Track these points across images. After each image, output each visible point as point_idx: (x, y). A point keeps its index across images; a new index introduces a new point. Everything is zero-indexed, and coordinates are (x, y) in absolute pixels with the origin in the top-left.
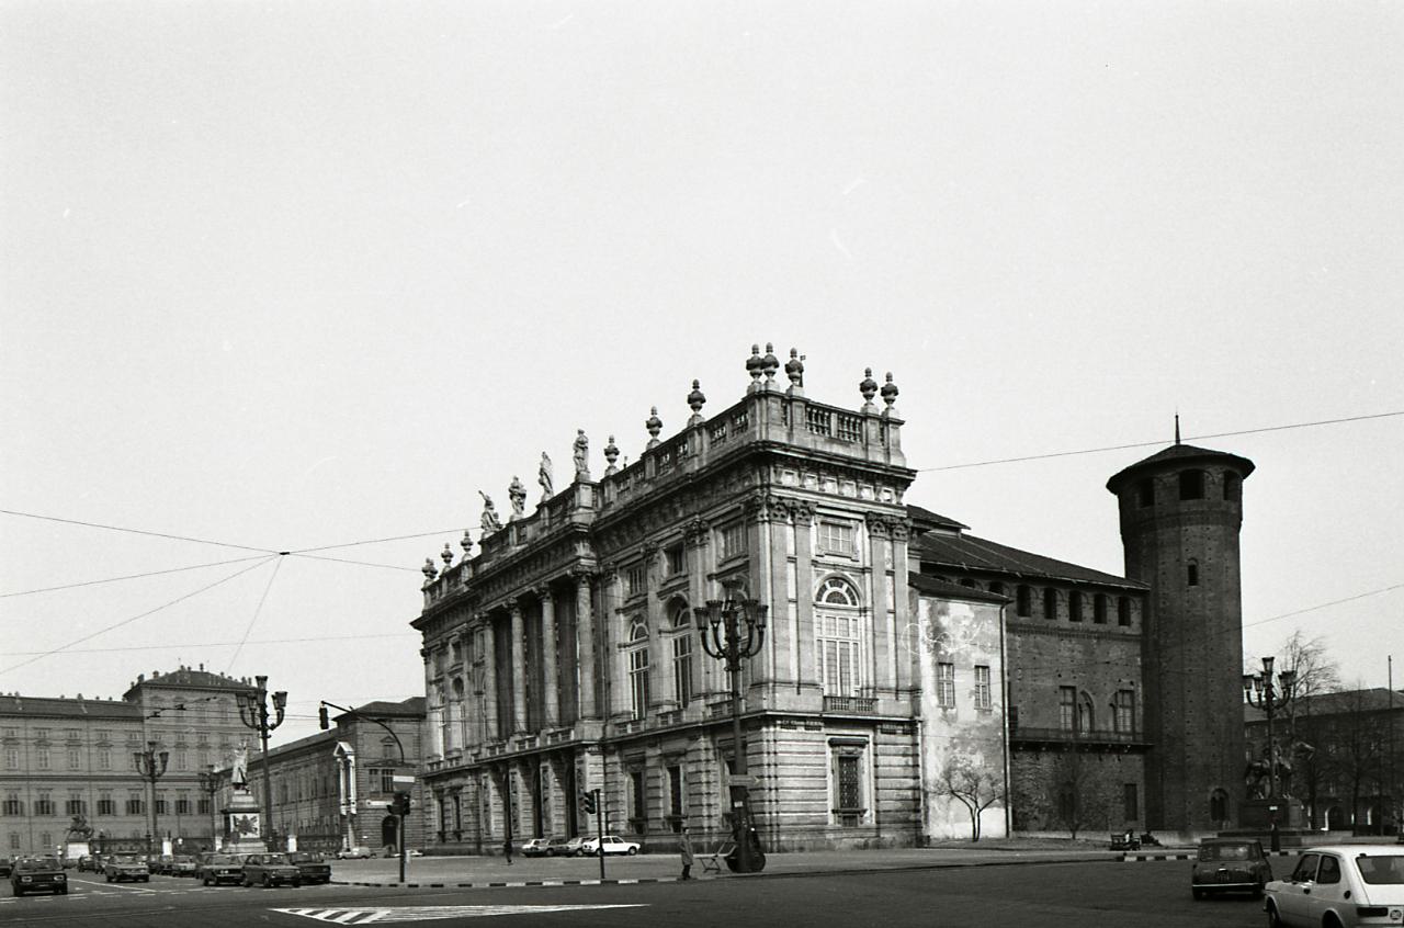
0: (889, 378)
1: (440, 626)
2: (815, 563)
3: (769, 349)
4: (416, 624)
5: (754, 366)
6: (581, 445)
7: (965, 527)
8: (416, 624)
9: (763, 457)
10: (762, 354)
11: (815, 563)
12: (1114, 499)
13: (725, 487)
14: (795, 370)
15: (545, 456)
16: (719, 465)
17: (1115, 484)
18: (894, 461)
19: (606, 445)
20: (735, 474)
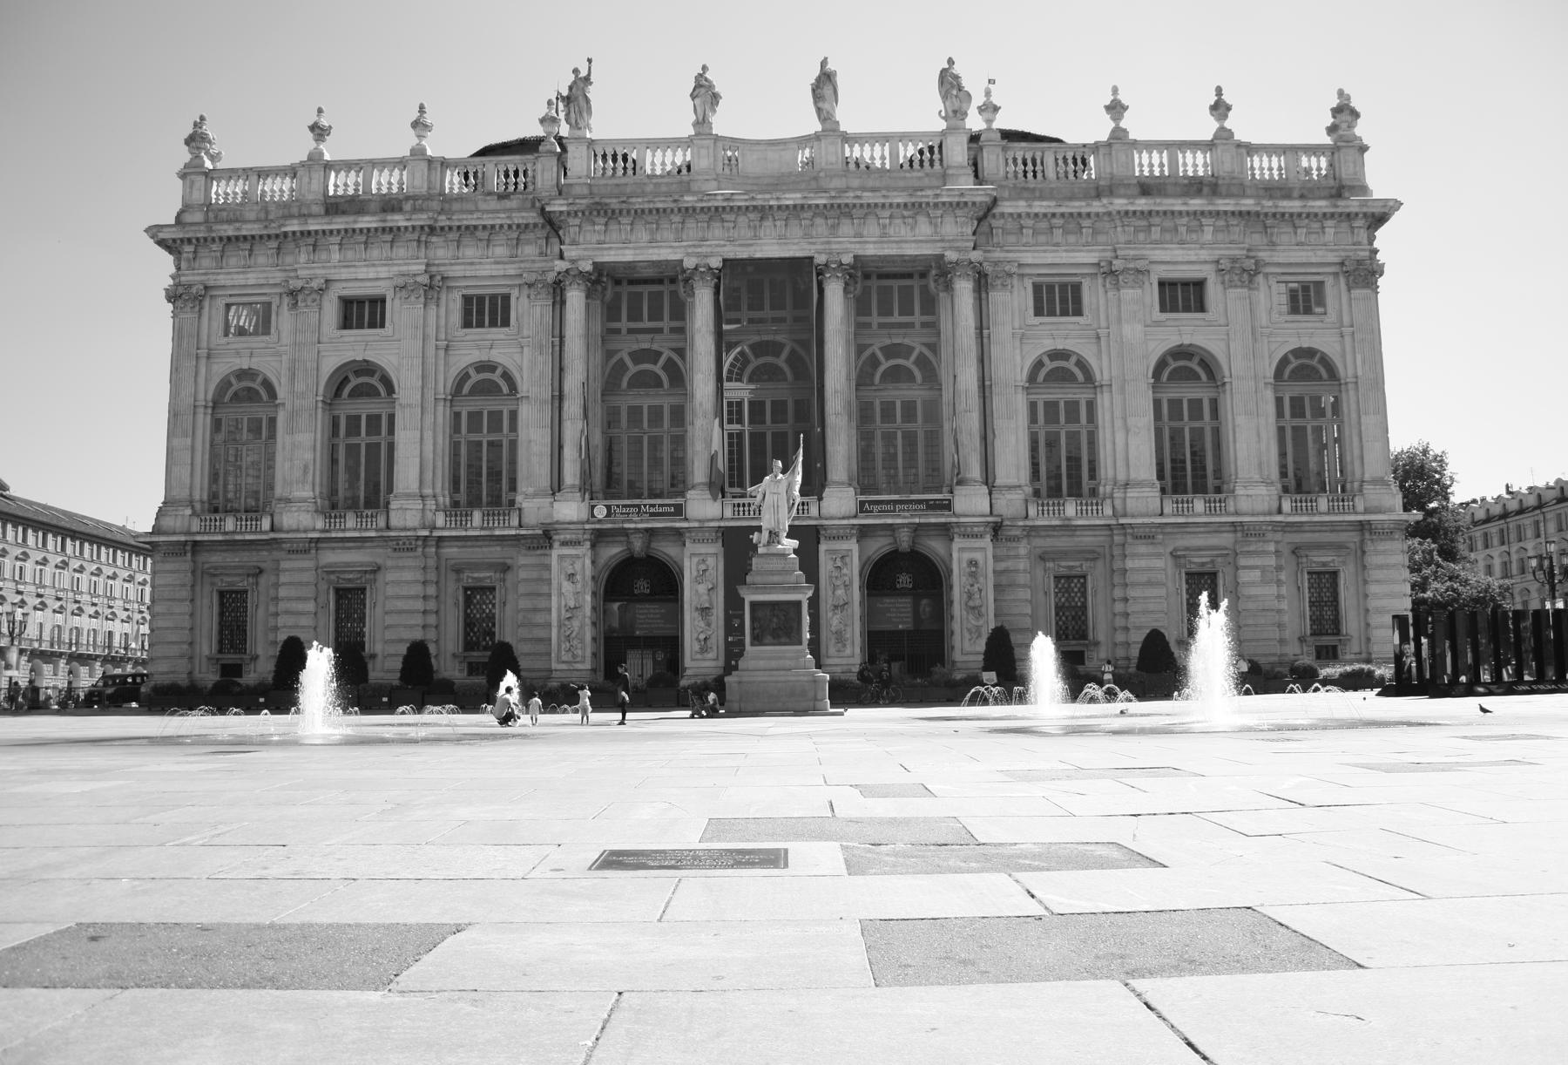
3: (1349, 98)
6: (949, 82)
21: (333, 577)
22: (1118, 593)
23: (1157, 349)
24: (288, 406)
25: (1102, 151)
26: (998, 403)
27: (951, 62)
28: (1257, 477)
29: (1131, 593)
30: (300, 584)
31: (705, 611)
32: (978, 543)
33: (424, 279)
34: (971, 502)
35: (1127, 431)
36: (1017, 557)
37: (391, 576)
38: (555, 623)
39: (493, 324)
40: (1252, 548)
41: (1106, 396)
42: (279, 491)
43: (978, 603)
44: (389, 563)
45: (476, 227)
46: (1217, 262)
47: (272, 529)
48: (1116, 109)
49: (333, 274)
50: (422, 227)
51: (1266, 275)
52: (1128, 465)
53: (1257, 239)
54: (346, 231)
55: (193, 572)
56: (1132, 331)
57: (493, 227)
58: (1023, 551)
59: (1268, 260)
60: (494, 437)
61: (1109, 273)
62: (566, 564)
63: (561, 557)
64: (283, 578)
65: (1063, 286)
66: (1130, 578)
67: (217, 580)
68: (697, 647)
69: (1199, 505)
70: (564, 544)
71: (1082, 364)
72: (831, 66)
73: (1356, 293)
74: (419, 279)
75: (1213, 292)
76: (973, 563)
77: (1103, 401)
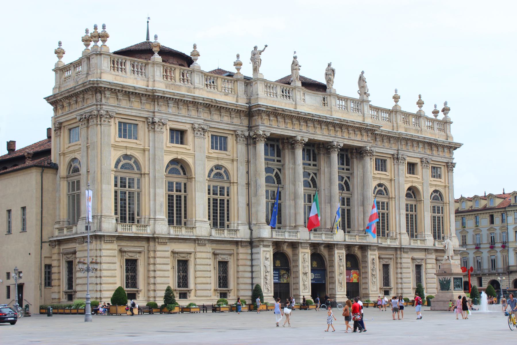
21: (176, 255)
22: (399, 270)
23: (407, 186)
24: (151, 175)
25: (394, 113)
27: (363, 73)
29: (404, 270)
30: (164, 258)
31: (305, 274)
32: (374, 253)
35: (400, 214)
38: (262, 277)
39: (221, 149)
40: (430, 257)
41: (393, 202)
42: (145, 213)
44: (198, 250)
45: (223, 108)
46: (421, 158)
48: (396, 98)
50: (207, 104)
52: (400, 227)
53: (428, 152)
54: (179, 99)
56: (402, 179)
57: (230, 108)
60: (222, 197)
61: (396, 158)
62: (265, 253)
63: (264, 251)
64: (158, 254)
65: (382, 160)
66: (404, 265)
67: (124, 254)
68: (303, 288)
70: (265, 246)
72: (332, 66)
73: (450, 173)
74: (202, 126)
75: (419, 167)
77: (392, 204)
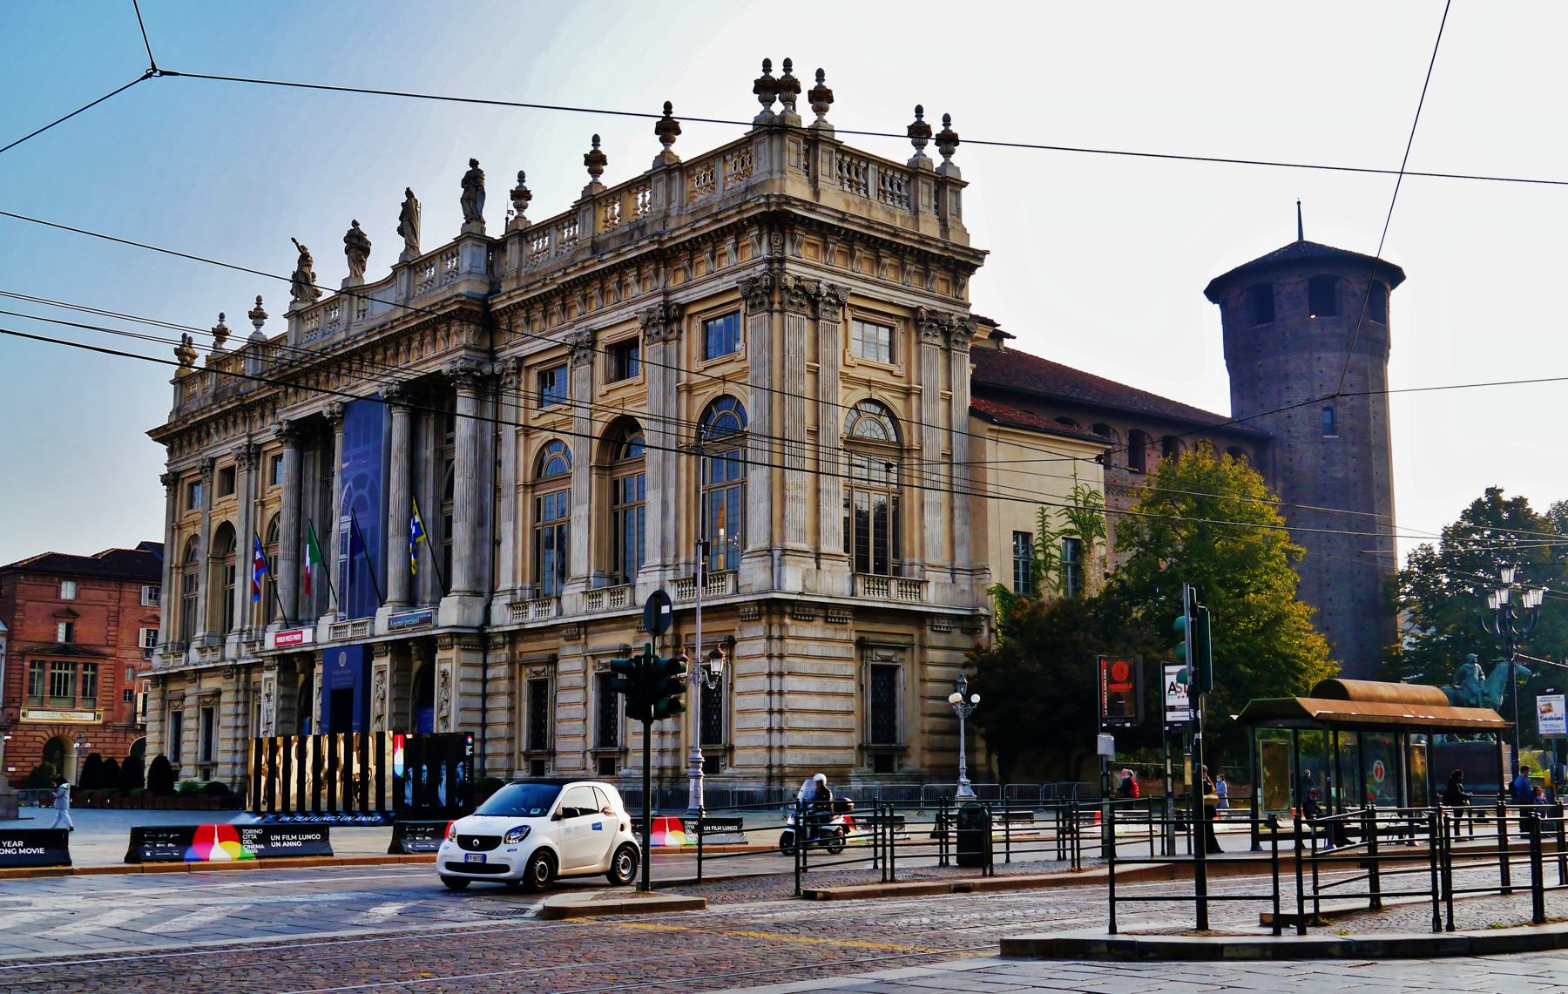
0: (947, 120)
1: (200, 440)
2: (846, 378)
3: (788, 64)
4: (158, 435)
5: (766, 88)
6: (473, 184)
7: (1008, 336)
8: (158, 435)
9: (780, 221)
10: (777, 73)
11: (846, 378)
12: (1216, 309)
13: (713, 259)
14: (821, 98)
15: (409, 193)
16: (707, 226)
17: (1217, 290)
18: (954, 238)
19: (515, 184)
20: (731, 241)
26: (505, 506)
28: (658, 561)
33: (244, 450)
34: (450, 613)
36: (500, 664)
37: (224, 698)
43: (444, 713)
47: (187, 664)
49: (212, 453)
51: (691, 316)
53: (681, 276)
55: (163, 699)
58: (503, 658)
59: (684, 301)
69: (606, 598)
70: (269, 668)
71: (566, 451)
76: (445, 674)
